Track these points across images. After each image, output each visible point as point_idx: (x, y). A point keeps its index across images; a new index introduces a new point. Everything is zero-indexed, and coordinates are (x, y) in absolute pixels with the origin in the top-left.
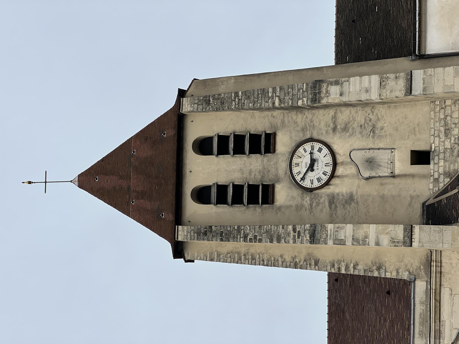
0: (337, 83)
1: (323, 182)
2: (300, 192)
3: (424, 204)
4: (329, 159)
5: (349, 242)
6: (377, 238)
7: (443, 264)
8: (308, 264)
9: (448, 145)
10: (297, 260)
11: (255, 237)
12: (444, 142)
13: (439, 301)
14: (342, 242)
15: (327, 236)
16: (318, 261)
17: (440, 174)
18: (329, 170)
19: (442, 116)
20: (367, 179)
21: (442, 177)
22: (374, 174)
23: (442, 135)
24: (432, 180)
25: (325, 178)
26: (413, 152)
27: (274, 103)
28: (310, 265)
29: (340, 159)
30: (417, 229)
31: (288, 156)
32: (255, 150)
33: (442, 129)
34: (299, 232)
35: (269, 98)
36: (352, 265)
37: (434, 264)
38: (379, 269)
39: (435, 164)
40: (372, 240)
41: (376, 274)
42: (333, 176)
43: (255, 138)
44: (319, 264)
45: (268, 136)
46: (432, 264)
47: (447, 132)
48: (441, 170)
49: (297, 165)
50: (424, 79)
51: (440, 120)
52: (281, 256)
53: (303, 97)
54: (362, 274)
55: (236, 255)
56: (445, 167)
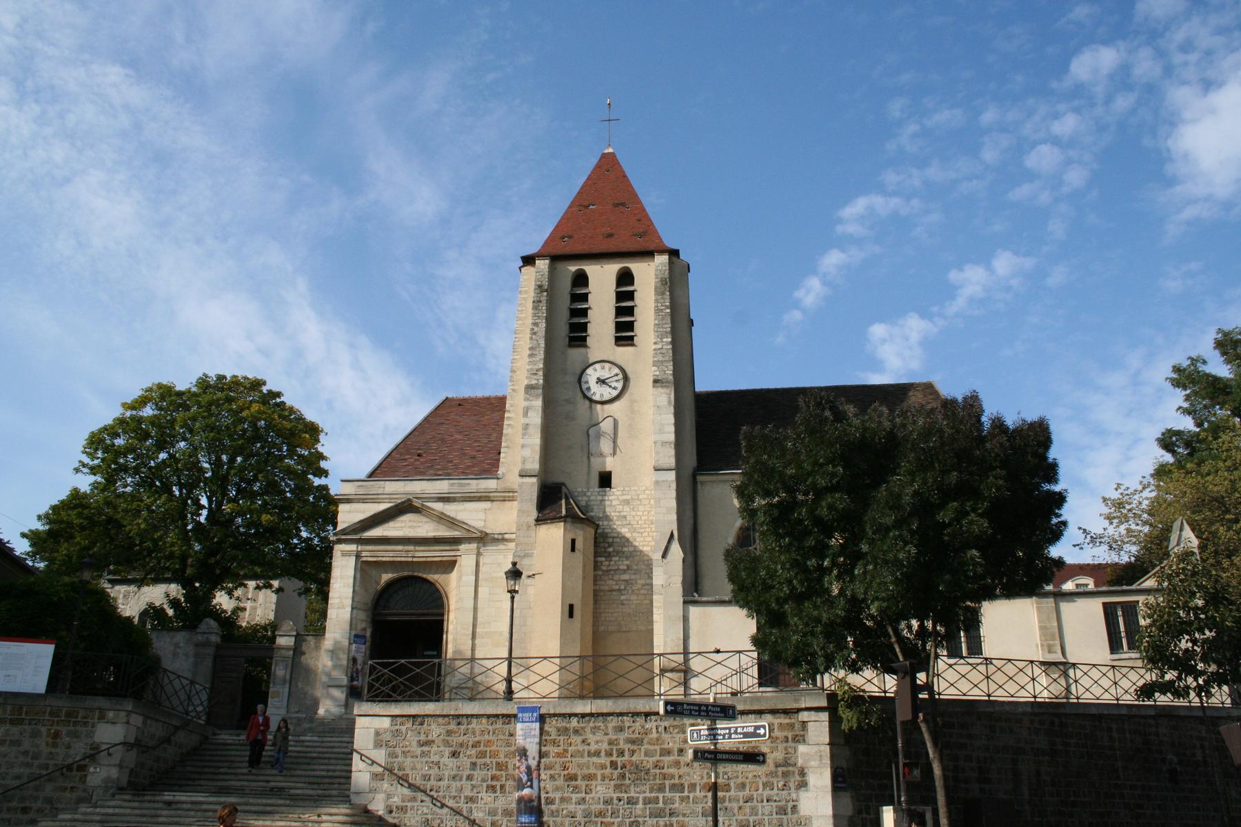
0: (669, 402)
1: (586, 393)
2: (578, 372)
3: (563, 484)
5: (526, 421)
9: (614, 503)
11: (535, 333)
12: (618, 499)
13: (479, 499)
14: (526, 414)
17: (589, 497)
19: (641, 497)
20: (588, 432)
21: (587, 499)
24: (585, 490)
26: (610, 473)
29: (606, 407)
31: (611, 359)
32: (620, 327)
33: (629, 497)
34: (536, 374)
35: (661, 339)
36: (512, 423)
37: (511, 494)
39: (599, 492)
40: (527, 441)
41: (503, 444)
43: (630, 326)
45: (632, 338)
47: (627, 502)
48: (592, 498)
49: (603, 368)
50: (666, 481)
51: (638, 495)
52: (522, 358)
54: (504, 432)
55: (524, 315)
56: (596, 501)
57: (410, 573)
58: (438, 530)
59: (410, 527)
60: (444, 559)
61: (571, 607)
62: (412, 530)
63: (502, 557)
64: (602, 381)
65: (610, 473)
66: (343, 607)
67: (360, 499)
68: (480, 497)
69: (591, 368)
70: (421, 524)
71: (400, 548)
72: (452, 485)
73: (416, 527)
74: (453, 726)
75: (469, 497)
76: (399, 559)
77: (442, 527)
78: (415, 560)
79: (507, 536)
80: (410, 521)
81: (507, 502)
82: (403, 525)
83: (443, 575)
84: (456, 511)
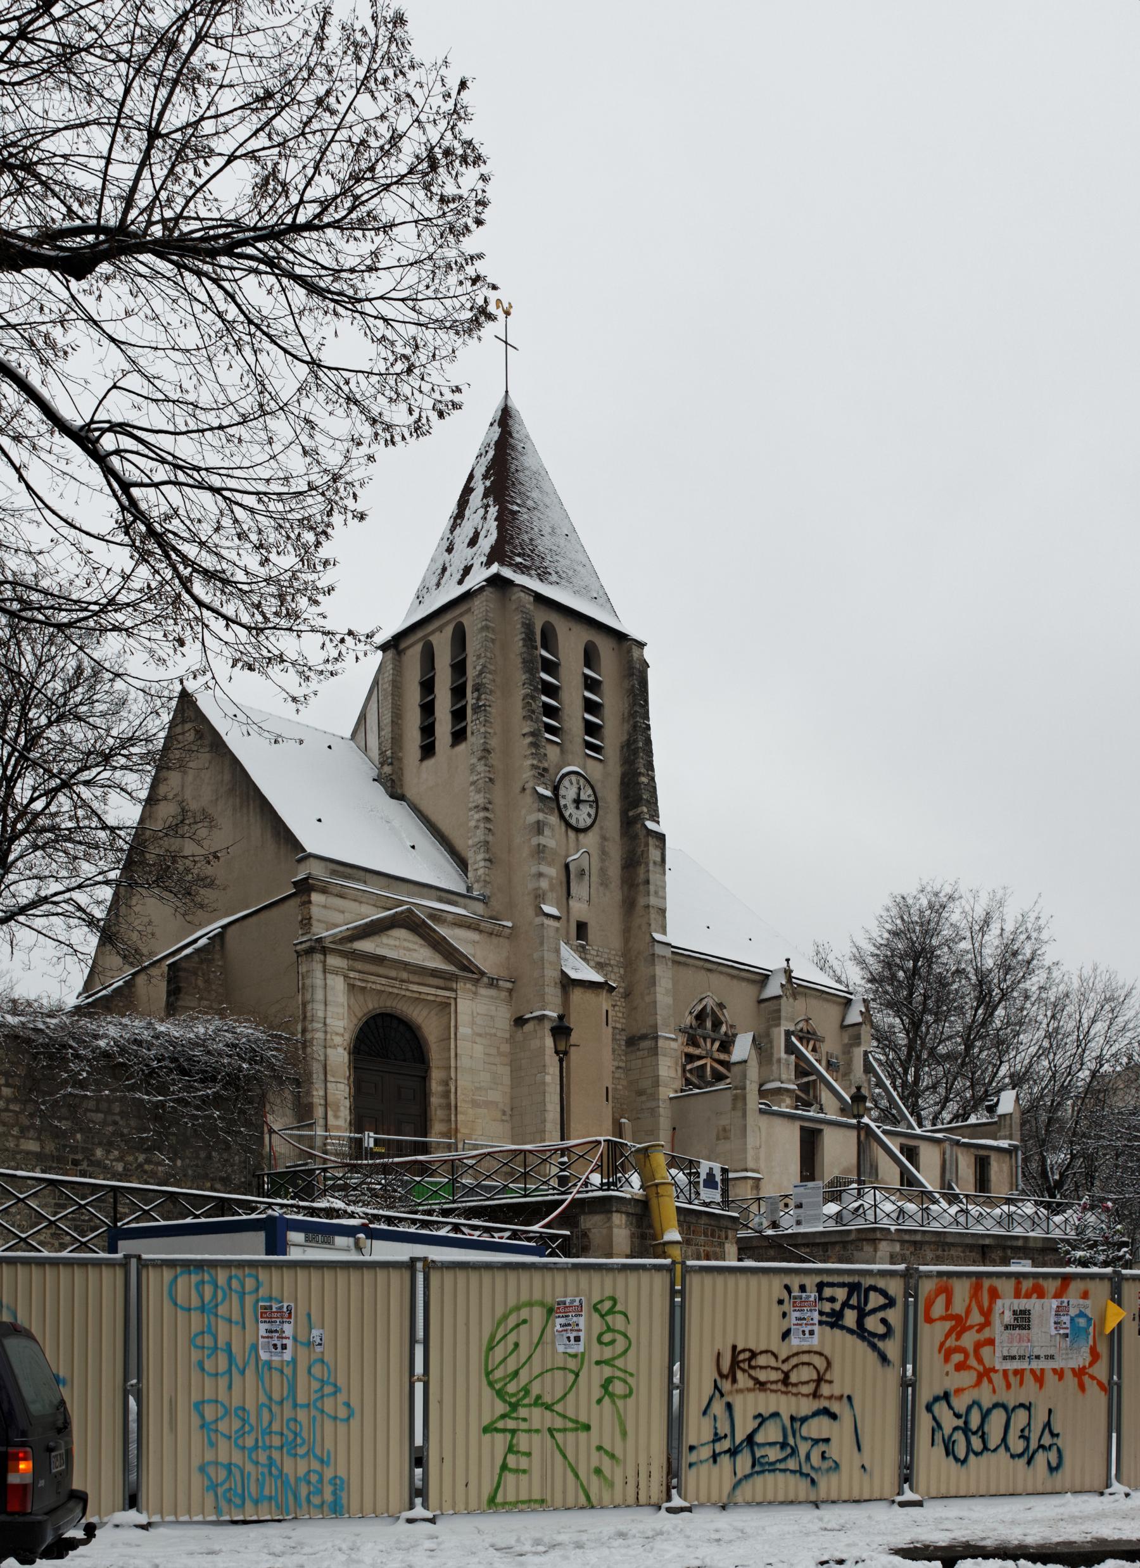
4: (582, 825)
18: (573, 822)
19: (612, 962)
20: (567, 866)
22: (572, 876)
23: (598, 959)
25: (567, 814)
27: (643, 775)
29: (581, 836)
30: (556, 924)
33: (602, 960)
38: (490, 860)
42: (568, 825)
50: (664, 957)
59: (404, 949)
63: (493, 1008)
64: (578, 802)
69: (567, 778)
70: (416, 947)
71: (393, 974)
73: (409, 950)
74: (940, 1253)
76: (391, 990)
77: (437, 956)
78: (408, 994)
82: (397, 943)
84: (458, 939)
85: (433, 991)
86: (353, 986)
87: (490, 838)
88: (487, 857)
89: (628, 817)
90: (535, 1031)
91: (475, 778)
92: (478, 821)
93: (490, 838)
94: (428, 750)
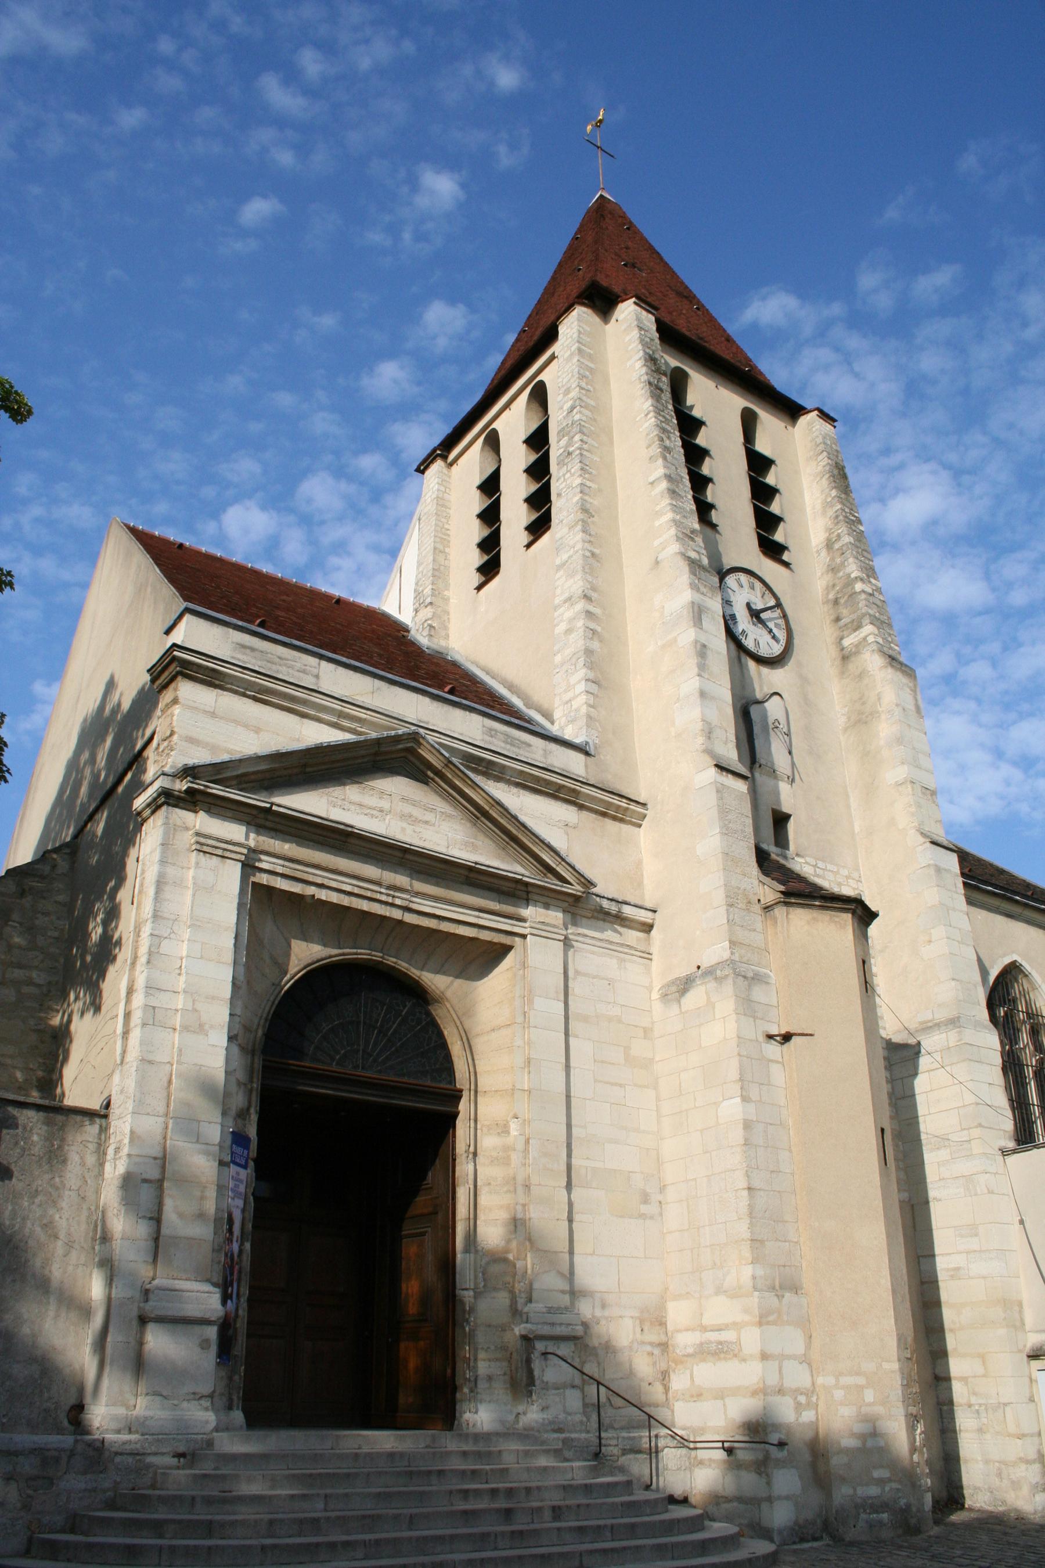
4: (764, 652)
6: (713, 698)
7: (617, 824)
8: (592, 539)
10: (595, 519)
15: (703, 594)
16: (598, 561)
28: (590, 541)
35: (868, 576)
36: (599, 629)
37: (623, 804)
44: (591, 561)
46: (624, 800)
50: (947, 871)
52: (600, 490)
53: (883, 639)
57: (377, 956)
58: (475, 848)
59: (403, 817)
60: (485, 936)
61: (882, 1130)
62: (409, 829)
65: (787, 817)
66: (201, 1029)
67: (251, 685)
68: (560, 788)
70: (429, 816)
71: (371, 871)
72: (491, 732)
73: (416, 821)
75: (538, 780)
76: (365, 906)
78: (410, 918)
79: (627, 910)
80: (404, 799)
81: (608, 822)
82: (385, 804)
83: (459, 982)
85: (471, 917)
86: (270, 890)
87: (595, 645)
88: (591, 675)
89: (842, 649)
90: (711, 1005)
91: (565, 557)
92: (571, 620)
93: (595, 645)
94: (490, 569)
